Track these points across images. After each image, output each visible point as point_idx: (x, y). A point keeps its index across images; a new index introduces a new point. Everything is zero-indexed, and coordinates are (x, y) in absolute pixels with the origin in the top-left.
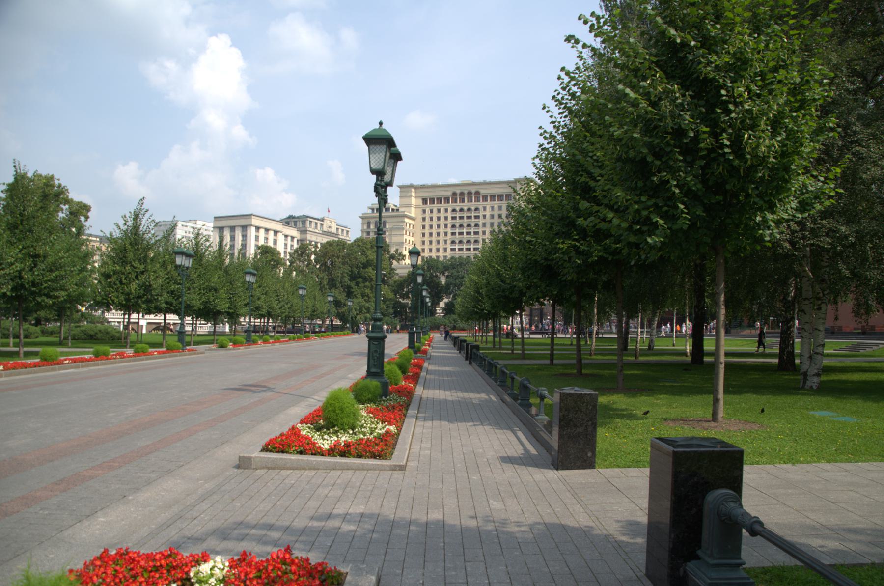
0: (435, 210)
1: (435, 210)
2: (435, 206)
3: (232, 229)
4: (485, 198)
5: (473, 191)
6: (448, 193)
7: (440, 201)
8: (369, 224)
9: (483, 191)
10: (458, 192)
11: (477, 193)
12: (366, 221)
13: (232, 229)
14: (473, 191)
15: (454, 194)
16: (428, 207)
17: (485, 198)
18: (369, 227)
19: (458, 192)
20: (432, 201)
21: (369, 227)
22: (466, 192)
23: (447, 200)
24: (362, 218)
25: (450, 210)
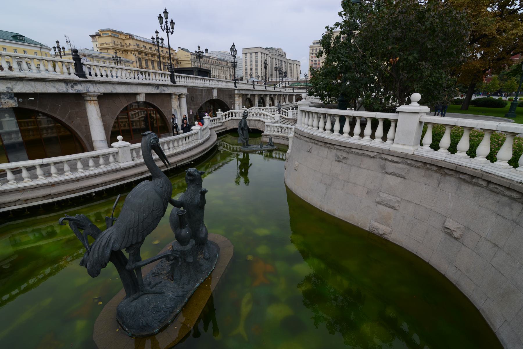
3: (251, 53)
8: (313, 50)
12: (311, 48)
13: (251, 53)
18: (313, 51)
21: (313, 51)
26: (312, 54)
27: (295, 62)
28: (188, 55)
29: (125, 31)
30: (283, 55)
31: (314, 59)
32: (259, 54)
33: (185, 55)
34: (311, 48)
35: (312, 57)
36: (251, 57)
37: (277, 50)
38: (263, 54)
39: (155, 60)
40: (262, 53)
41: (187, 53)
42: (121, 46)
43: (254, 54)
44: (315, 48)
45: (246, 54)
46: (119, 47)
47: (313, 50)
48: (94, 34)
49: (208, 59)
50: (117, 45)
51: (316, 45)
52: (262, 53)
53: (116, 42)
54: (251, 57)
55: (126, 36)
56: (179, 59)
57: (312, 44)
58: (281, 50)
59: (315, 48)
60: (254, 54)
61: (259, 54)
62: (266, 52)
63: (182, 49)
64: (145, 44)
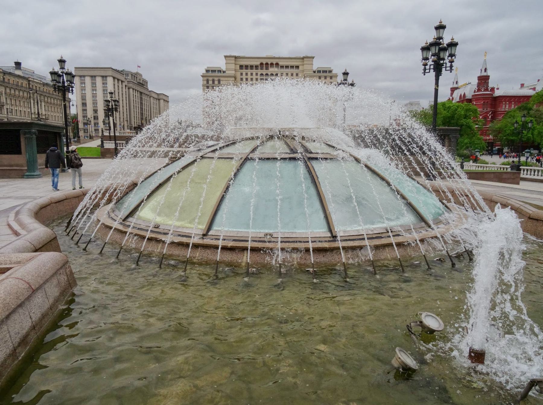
0: (249, 74)
1: (249, 74)
2: (249, 71)
3: (93, 77)
4: (282, 67)
5: (274, 63)
6: (258, 63)
7: (252, 67)
8: (208, 81)
9: (281, 63)
10: (264, 63)
11: (277, 64)
12: (206, 78)
14: (274, 63)
15: (262, 64)
16: (244, 71)
17: (282, 67)
19: (264, 63)
20: (247, 67)
22: (269, 63)
23: (257, 67)
24: (203, 76)
25: (259, 74)
27: (161, 97)
30: (143, 84)
34: (206, 78)
36: (94, 84)
37: (135, 75)
38: (116, 81)
40: (114, 78)
43: (99, 80)
44: (211, 79)
47: (208, 81)
49: (25, 83)
51: (210, 74)
54: (94, 84)
57: (204, 72)
58: (141, 75)
59: (211, 79)
61: (110, 80)
62: (122, 78)
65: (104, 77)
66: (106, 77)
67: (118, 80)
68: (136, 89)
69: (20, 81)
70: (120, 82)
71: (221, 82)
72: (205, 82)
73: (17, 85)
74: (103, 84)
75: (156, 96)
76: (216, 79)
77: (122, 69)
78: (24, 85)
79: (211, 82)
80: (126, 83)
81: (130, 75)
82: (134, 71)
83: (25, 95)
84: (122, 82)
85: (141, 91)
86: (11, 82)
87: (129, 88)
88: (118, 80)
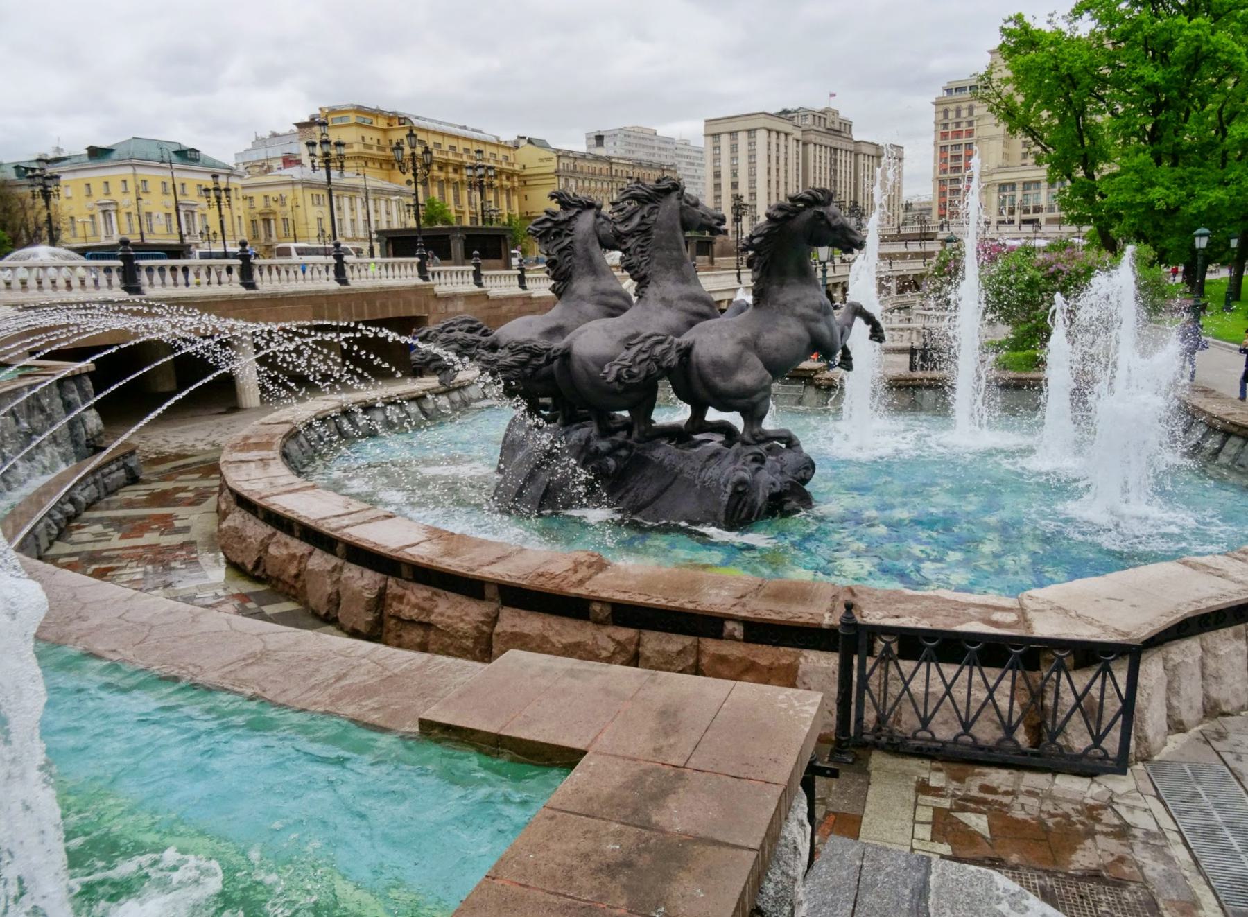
8: (946, 112)
12: (941, 108)
13: (733, 134)
18: (946, 116)
21: (946, 116)
24: (936, 104)
26: (946, 126)
28: (549, 159)
29: (387, 107)
30: (840, 130)
31: (950, 142)
32: (761, 136)
33: (541, 160)
35: (944, 136)
36: (734, 148)
37: (820, 116)
38: (774, 135)
39: (448, 180)
40: (769, 131)
41: (544, 153)
42: (379, 148)
43: (743, 138)
44: (952, 107)
45: (716, 136)
46: (375, 151)
48: (307, 120)
49: (606, 166)
50: (370, 147)
51: (956, 96)
52: (769, 131)
53: (367, 141)
54: (734, 148)
55: (390, 118)
56: (526, 172)
58: (835, 113)
60: (743, 137)
61: (761, 136)
62: (785, 126)
63: (530, 141)
64: (454, 142)
65: (751, 131)
66: (755, 130)
67: (778, 133)
68: (823, 142)
69: (598, 166)
70: (782, 136)
71: (976, 112)
72: (941, 116)
73: (594, 174)
74: (750, 144)
75: (872, 151)
76: (965, 105)
77: (796, 108)
78: (604, 172)
79: (952, 115)
80: (798, 134)
81: (810, 117)
82: (819, 107)
83: (605, 186)
84: (786, 134)
85: (834, 145)
86: (585, 170)
87: (805, 144)
88: (778, 133)
